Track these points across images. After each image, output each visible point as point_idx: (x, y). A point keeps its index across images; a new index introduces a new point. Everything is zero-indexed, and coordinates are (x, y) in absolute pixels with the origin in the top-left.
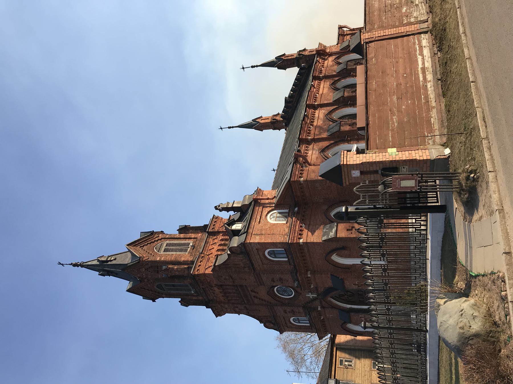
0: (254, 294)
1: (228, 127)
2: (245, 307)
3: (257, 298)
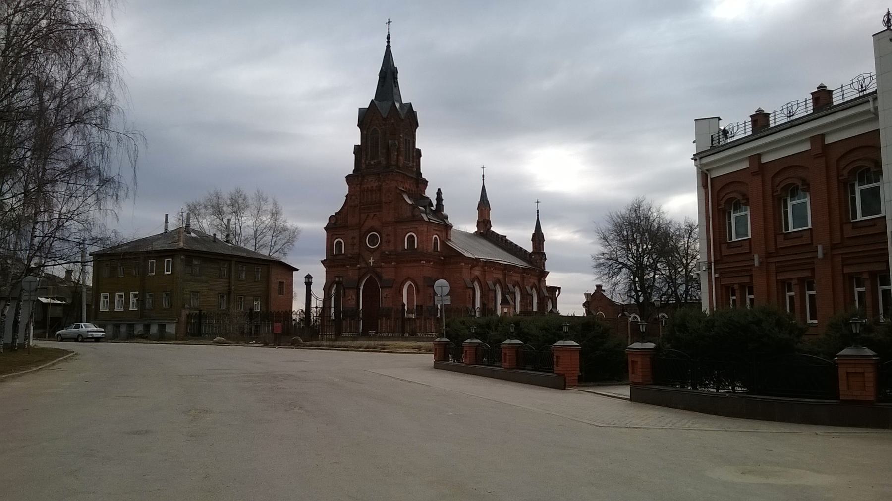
0: (372, 215)
1: (484, 174)
2: (357, 206)
3: (367, 217)
